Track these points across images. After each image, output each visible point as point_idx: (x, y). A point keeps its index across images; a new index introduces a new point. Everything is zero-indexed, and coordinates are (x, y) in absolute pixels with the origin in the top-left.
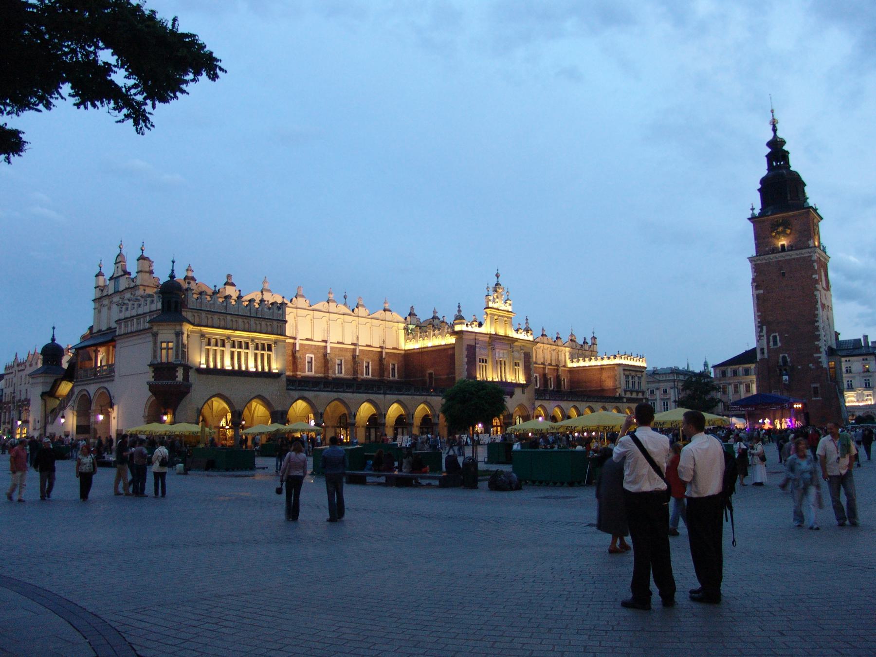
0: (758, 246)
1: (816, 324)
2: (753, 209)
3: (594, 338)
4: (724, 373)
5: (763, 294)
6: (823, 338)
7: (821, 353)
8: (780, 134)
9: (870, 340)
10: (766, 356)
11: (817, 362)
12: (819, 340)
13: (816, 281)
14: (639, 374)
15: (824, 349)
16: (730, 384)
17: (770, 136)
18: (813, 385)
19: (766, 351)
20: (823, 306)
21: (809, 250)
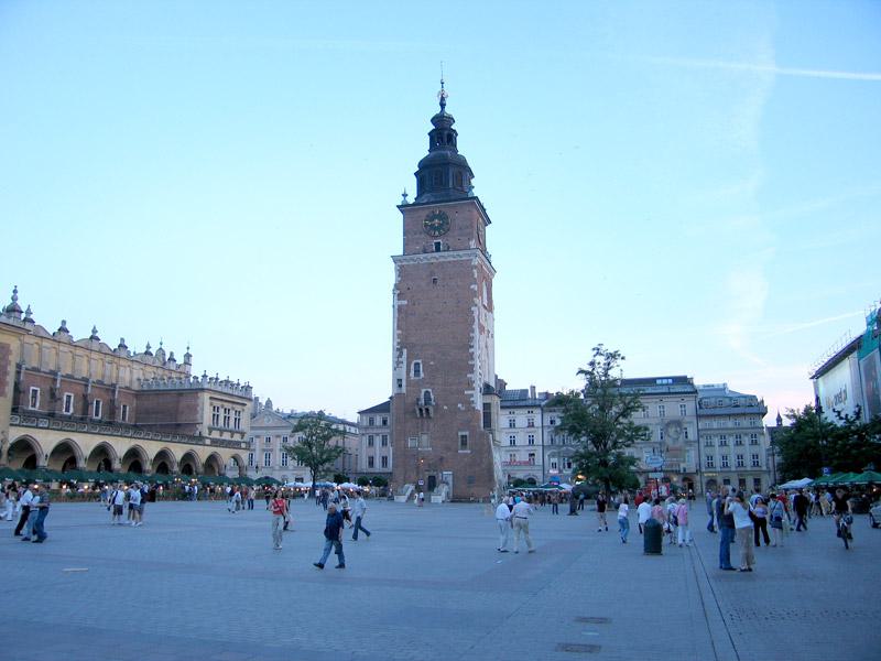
0: (406, 244)
1: (471, 350)
2: (405, 195)
3: (188, 356)
4: (371, 421)
5: (407, 305)
6: (477, 369)
7: (474, 389)
8: (448, 110)
9: (537, 391)
10: (404, 390)
11: (469, 403)
12: (472, 372)
13: (474, 294)
14: (238, 408)
15: (478, 385)
16: (377, 434)
17: (438, 110)
18: (460, 434)
19: (404, 383)
20: (482, 329)
21: (469, 252)
